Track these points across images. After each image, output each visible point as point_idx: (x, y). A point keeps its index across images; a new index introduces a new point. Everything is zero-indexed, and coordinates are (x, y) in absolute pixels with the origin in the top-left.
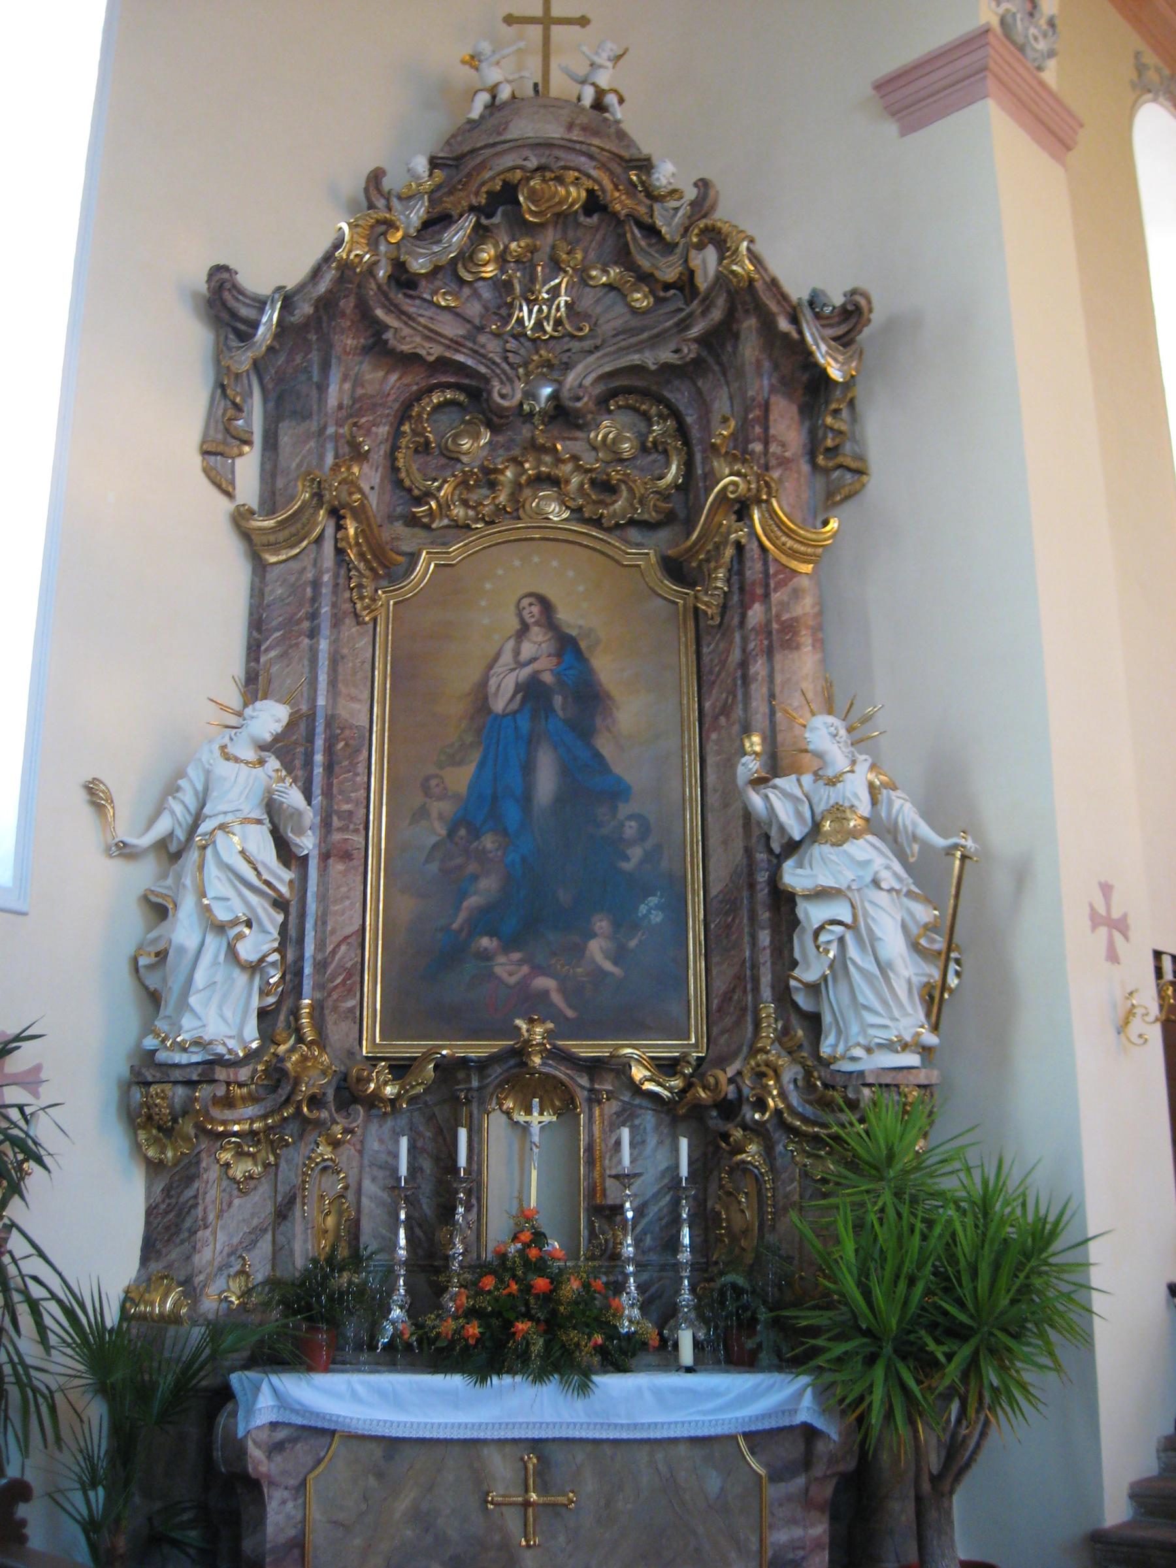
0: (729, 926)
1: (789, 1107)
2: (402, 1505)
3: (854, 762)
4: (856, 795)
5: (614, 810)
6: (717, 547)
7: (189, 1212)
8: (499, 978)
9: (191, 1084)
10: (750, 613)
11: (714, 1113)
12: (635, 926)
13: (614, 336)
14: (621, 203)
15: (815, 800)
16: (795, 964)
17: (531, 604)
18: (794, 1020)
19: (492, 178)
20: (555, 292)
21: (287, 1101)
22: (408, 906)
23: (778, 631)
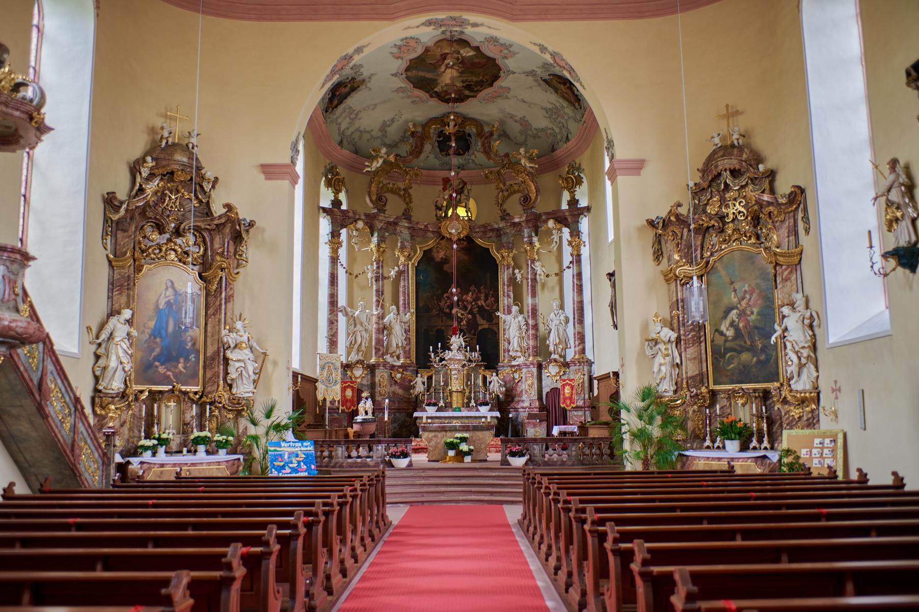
0: (212, 364)
6: (215, 276)
9: (112, 397)
12: (189, 360)
16: (229, 374)
18: (226, 385)
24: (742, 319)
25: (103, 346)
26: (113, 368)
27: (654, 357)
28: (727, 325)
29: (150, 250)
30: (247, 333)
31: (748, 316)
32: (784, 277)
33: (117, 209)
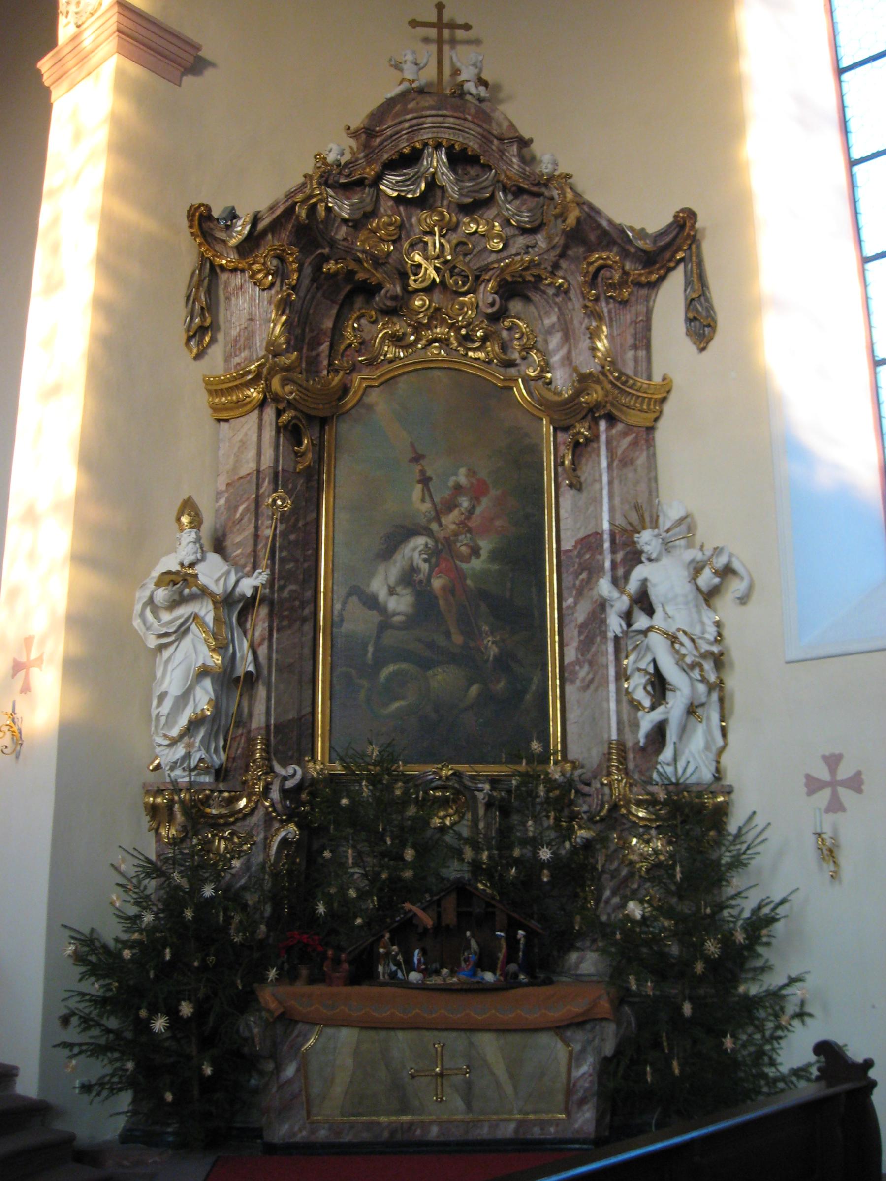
24: (443, 565)
27: (162, 647)
28: (392, 580)
31: (467, 560)
32: (620, 452)
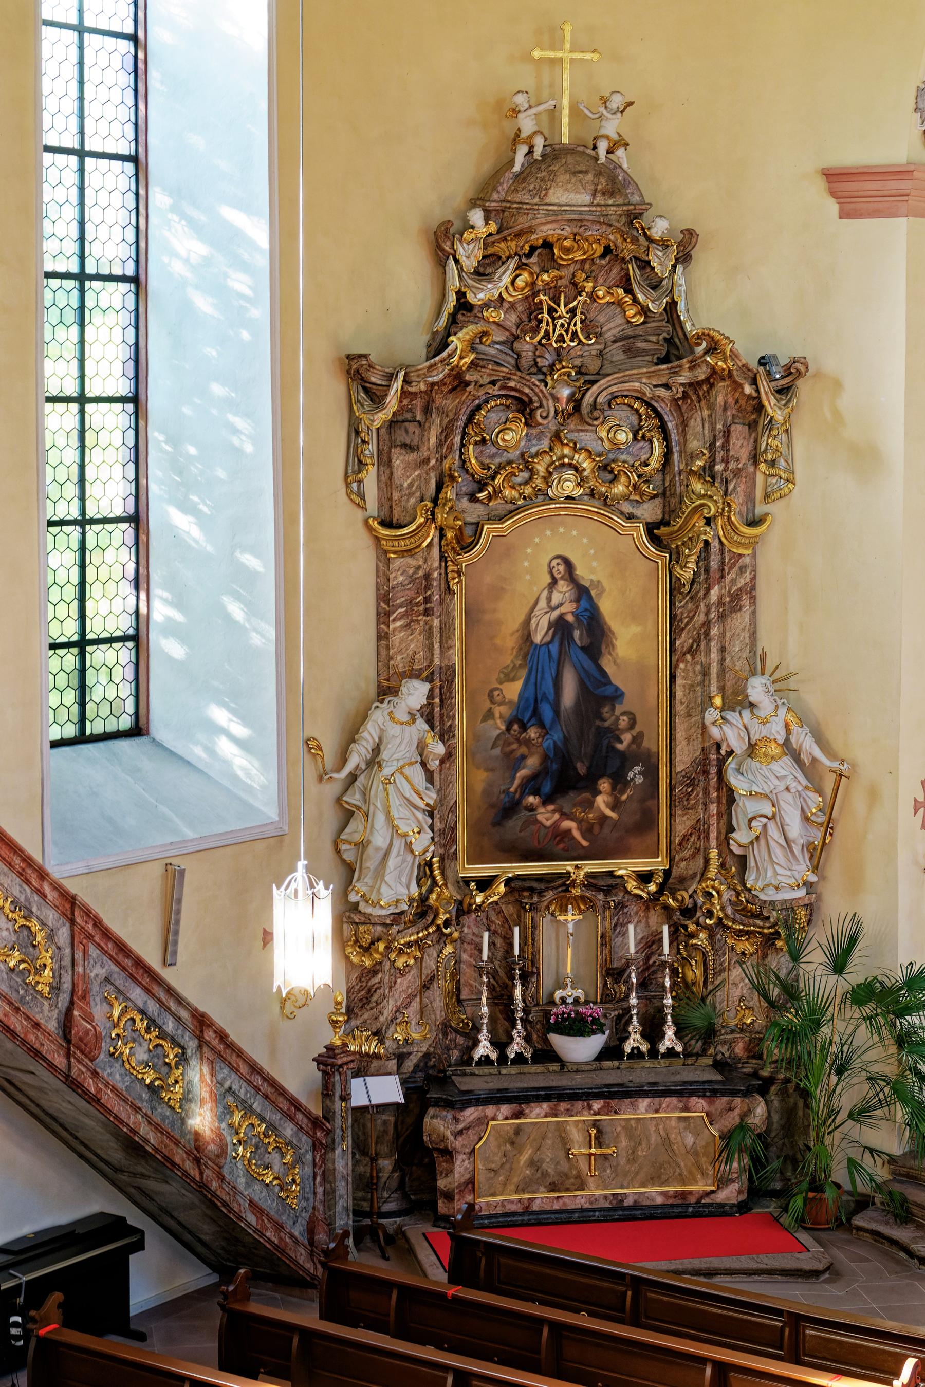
0: (689, 794)
1: (726, 915)
2: (524, 1157)
3: (777, 706)
4: (778, 732)
5: (613, 709)
7: (375, 991)
8: (540, 823)
10: (712, 592)
11: (678, 913)
13: (614, 342)
14: (627, 249)
15: (752, 733)
17: (558, 564)
18: (729, 860)
19: (537, 239)
20: (573, 312)
21: (433, 922)
22: (481, 777)
23: (729, 602)
25: (361, 779)
26: (378, 849)
29: (499, 480)
30: (782, 711)
33: (376, 397)
